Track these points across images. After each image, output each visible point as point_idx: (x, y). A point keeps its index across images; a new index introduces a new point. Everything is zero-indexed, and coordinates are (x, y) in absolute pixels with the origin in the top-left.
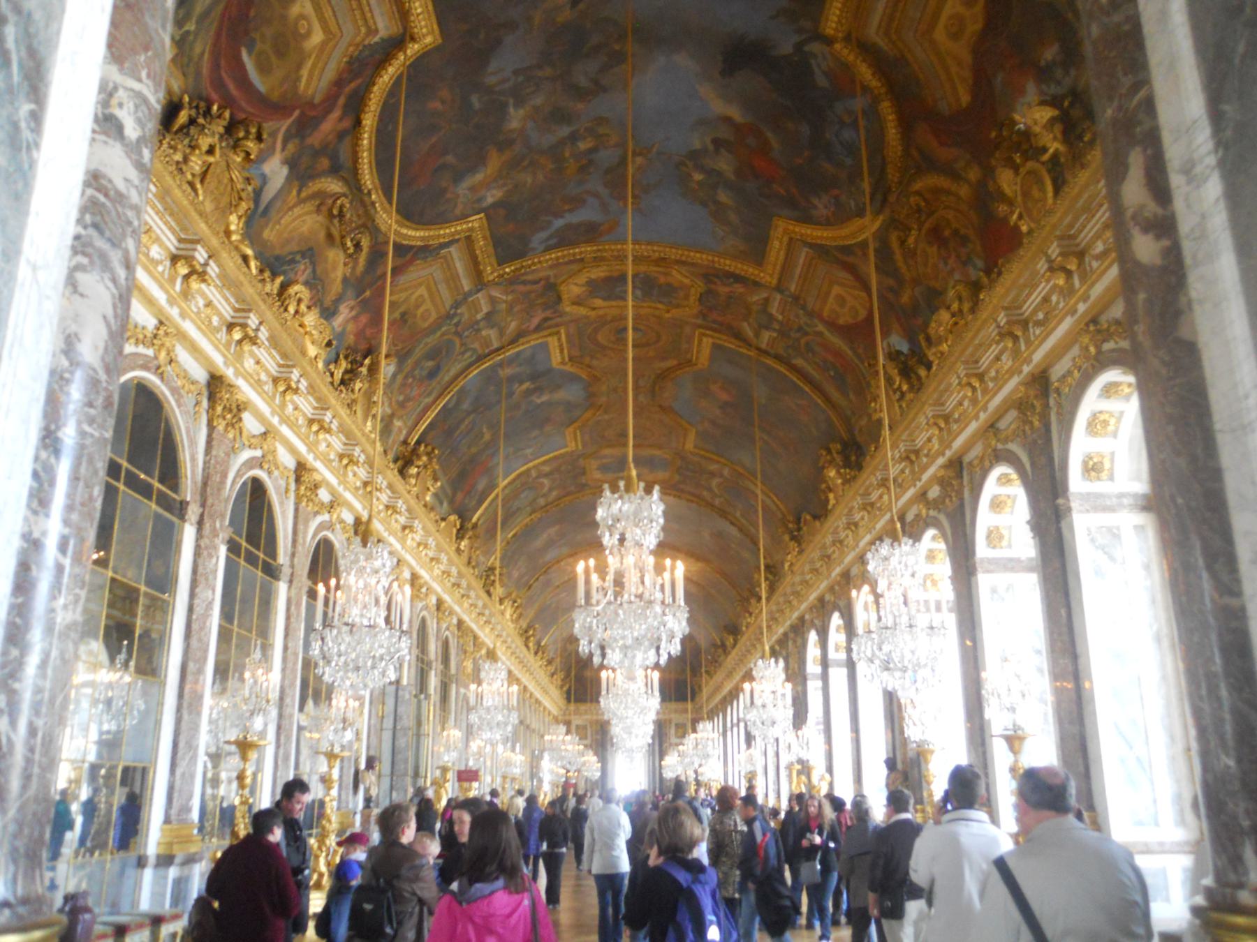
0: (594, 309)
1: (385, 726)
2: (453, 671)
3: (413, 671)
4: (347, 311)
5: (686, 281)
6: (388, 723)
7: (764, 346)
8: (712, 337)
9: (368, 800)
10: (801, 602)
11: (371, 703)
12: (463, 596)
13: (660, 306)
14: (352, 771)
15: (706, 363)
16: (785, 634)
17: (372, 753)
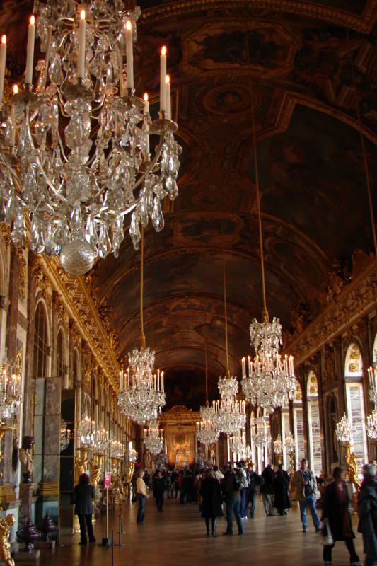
0: (206, 70)
1: (36, 414)
2: (79, 378)
3: (55, 370)
4: (9, 12)
5: (288, 38)
6: (39, 410)
7: (341, 104)
8: (296, 97)
9: (26, 476)
10: (336, 327)
11: (25, 391)
12: (85, 322)
13: (260, 68)
14: (12, 449)
15: (286, 127)
16: (319, 353)
17: (27, 434)
